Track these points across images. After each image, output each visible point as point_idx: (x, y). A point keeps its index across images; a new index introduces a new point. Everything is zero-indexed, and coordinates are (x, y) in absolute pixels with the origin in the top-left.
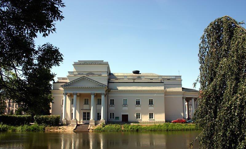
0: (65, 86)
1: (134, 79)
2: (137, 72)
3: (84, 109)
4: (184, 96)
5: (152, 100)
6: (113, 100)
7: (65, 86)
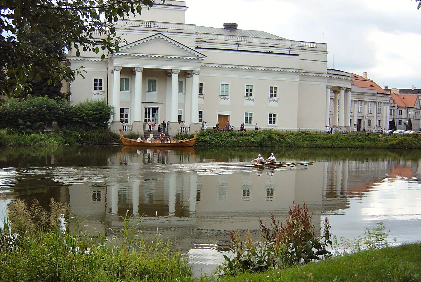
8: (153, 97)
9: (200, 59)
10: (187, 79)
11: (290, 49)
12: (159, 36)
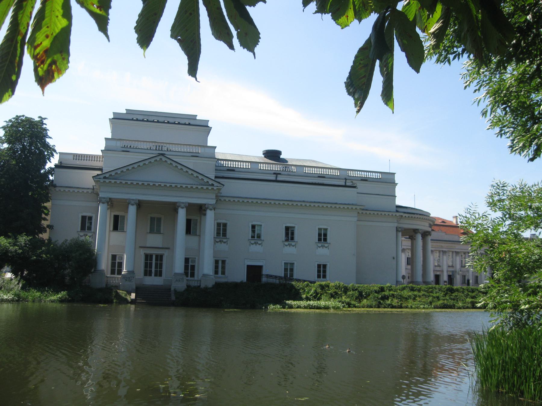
0: (105, 178)
1: (277, 174)
3: (148, 245)
4: (401, 225)
5: (326, 230)
6: (225, 225)
7: (105, 178)
8: (155, 240)
11: (346, 179)
12: (161, 159)
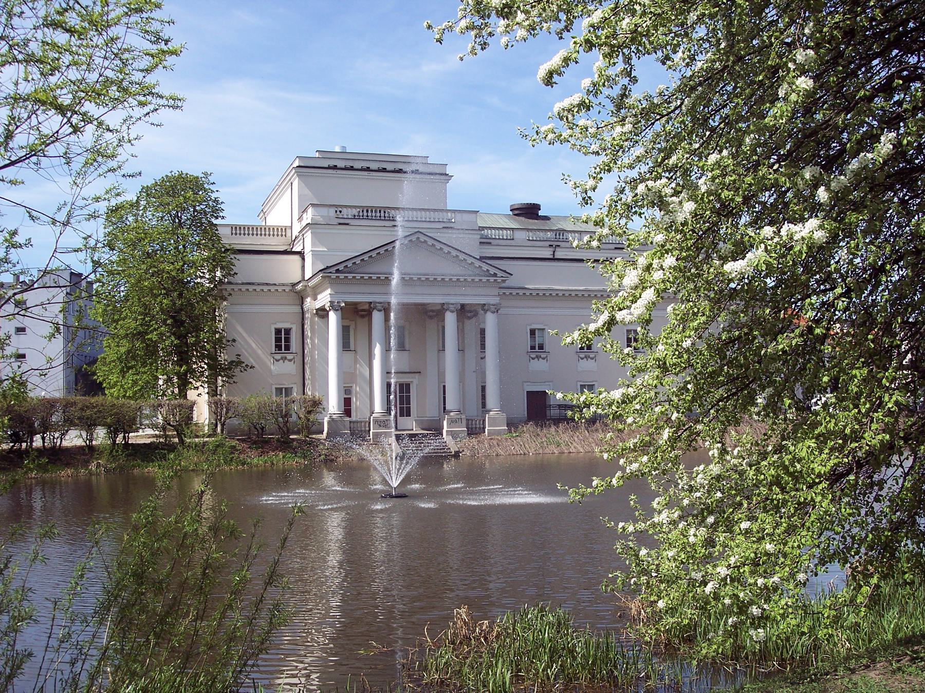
0: (338, 271)
2: (530, 211)
7: (338, 271)
9: (499, 280)
10: (466, 321)
